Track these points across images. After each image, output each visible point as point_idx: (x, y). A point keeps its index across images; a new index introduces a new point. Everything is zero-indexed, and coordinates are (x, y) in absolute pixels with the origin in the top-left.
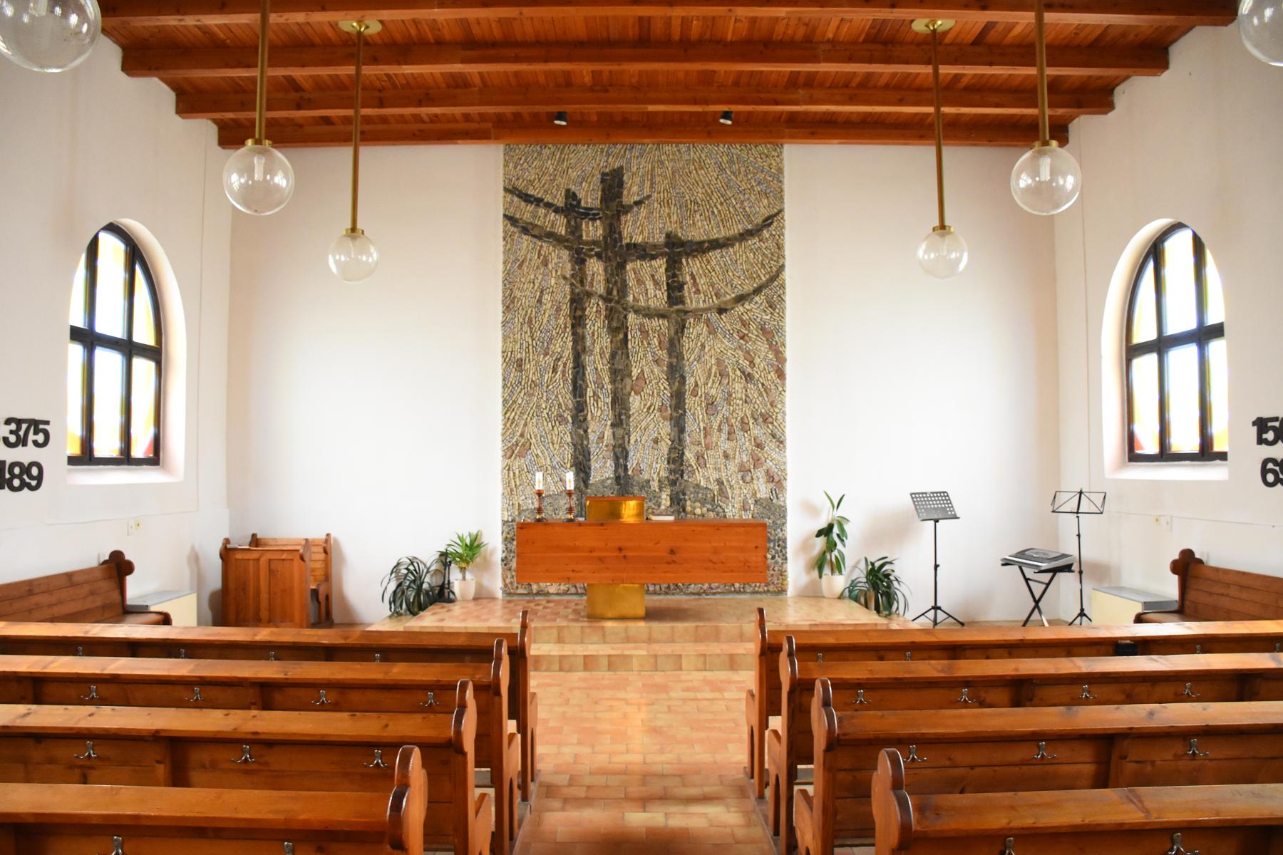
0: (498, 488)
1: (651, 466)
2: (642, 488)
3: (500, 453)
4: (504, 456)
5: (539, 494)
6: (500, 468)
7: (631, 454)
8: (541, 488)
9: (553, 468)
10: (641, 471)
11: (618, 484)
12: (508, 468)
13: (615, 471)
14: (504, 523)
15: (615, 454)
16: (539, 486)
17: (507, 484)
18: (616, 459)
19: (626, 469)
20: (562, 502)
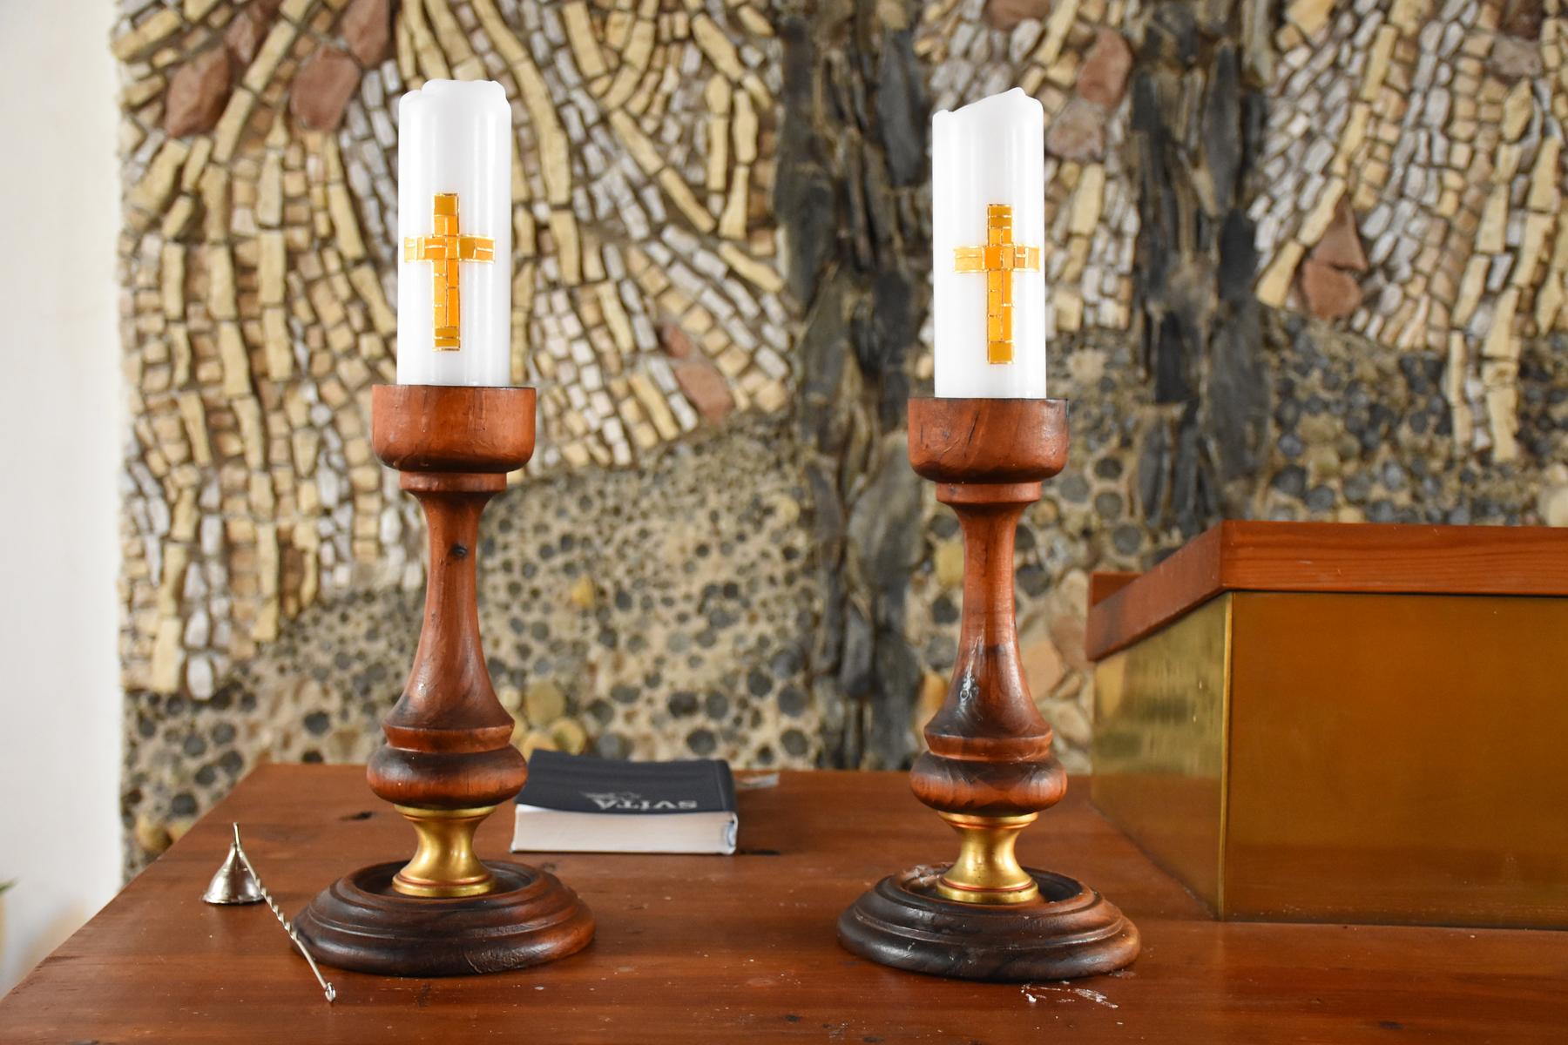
0: (98, 402)
1: (1457, 238)
2: (1371, 427)
3: (112, 81)
4: (147, 107)
5: (456, 465)
6: (111, 221)
7: (1288, 125)
8: (486, 360)
9: (601, 229)
10: (1372, 277)
11: (1170, 384)
12: (185, 220)
13: (1147, 277)
14: (150, 710)
15: (1150, 120)
16: (452, 328)
17: (172, 361)
18: (1156, 166)
19: (1236, 252)
20: (673, 539)
